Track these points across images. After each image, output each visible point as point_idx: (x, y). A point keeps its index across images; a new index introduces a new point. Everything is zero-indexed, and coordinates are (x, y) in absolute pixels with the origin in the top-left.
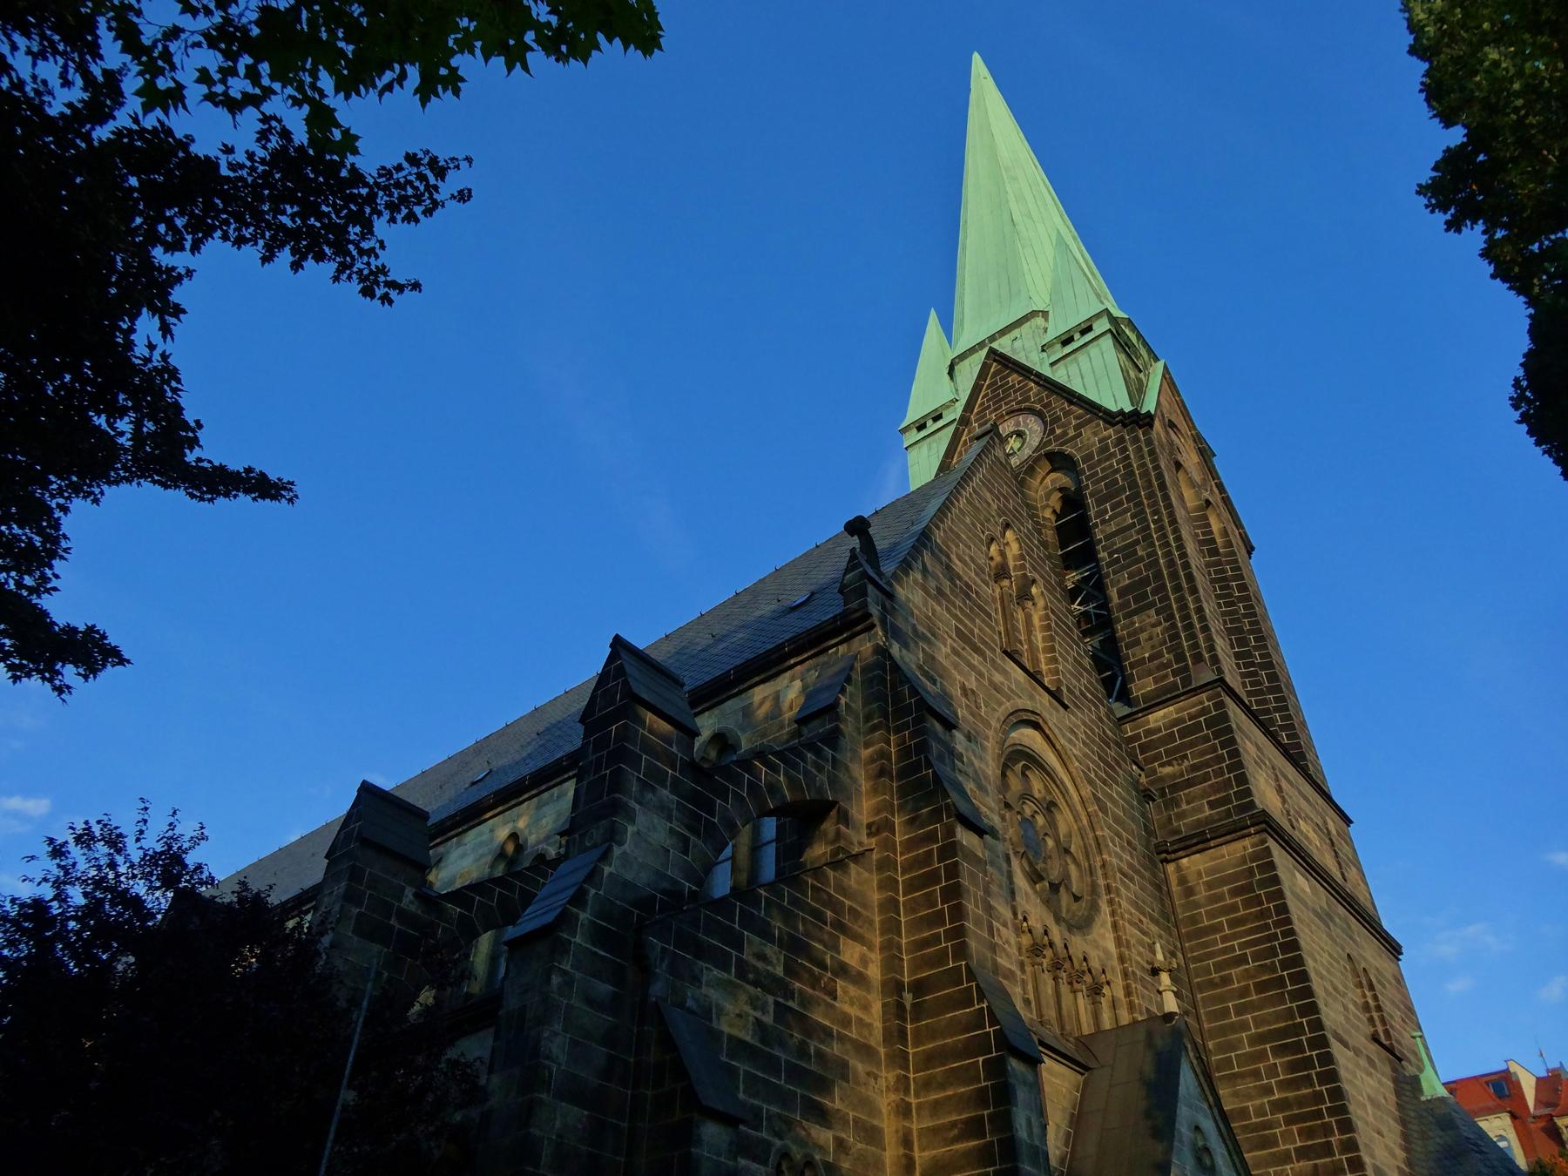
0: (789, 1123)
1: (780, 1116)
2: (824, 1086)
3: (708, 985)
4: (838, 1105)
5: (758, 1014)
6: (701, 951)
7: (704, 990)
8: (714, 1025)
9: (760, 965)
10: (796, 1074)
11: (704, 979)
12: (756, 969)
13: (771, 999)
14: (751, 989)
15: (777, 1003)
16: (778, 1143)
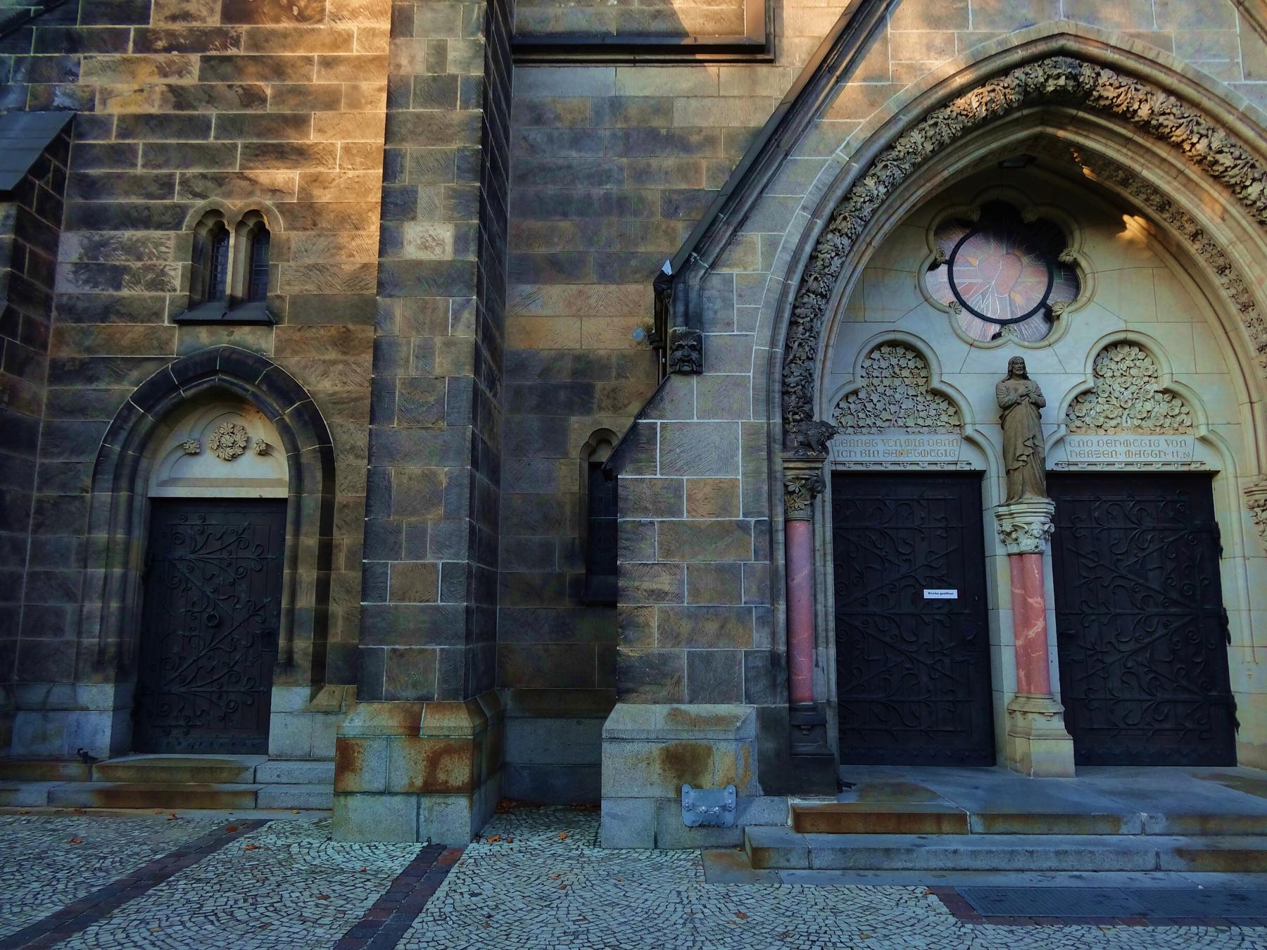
0: (220, 181)
1: (204, 176)
2: (299, 122)
3: (87, 74)
4: (313, 138)
5: (173, 80)
6: (75, 43)
7: (82, 81)
8: (99, 111)
9: (178, 26)
10: (231, 126)
11: (81, 71)
12: (171, 34)
13: (195, 58)
14: (161, 58)
15: (205, 60)
16: (200, 203)
